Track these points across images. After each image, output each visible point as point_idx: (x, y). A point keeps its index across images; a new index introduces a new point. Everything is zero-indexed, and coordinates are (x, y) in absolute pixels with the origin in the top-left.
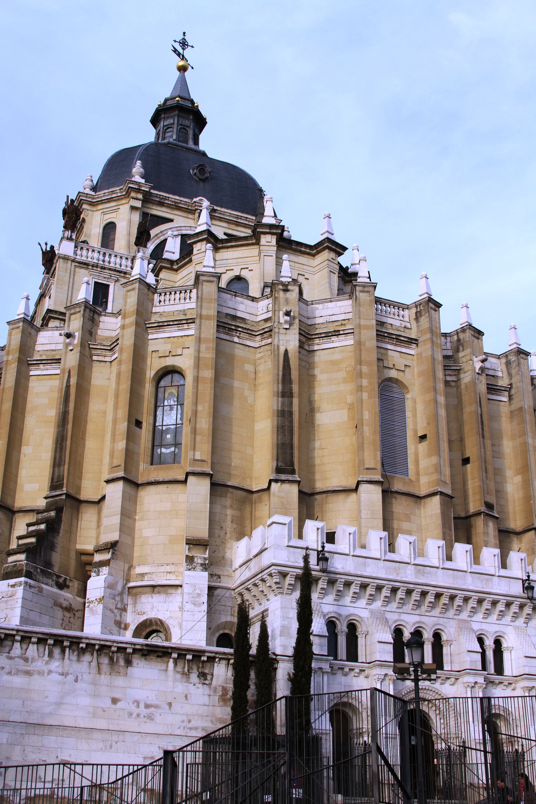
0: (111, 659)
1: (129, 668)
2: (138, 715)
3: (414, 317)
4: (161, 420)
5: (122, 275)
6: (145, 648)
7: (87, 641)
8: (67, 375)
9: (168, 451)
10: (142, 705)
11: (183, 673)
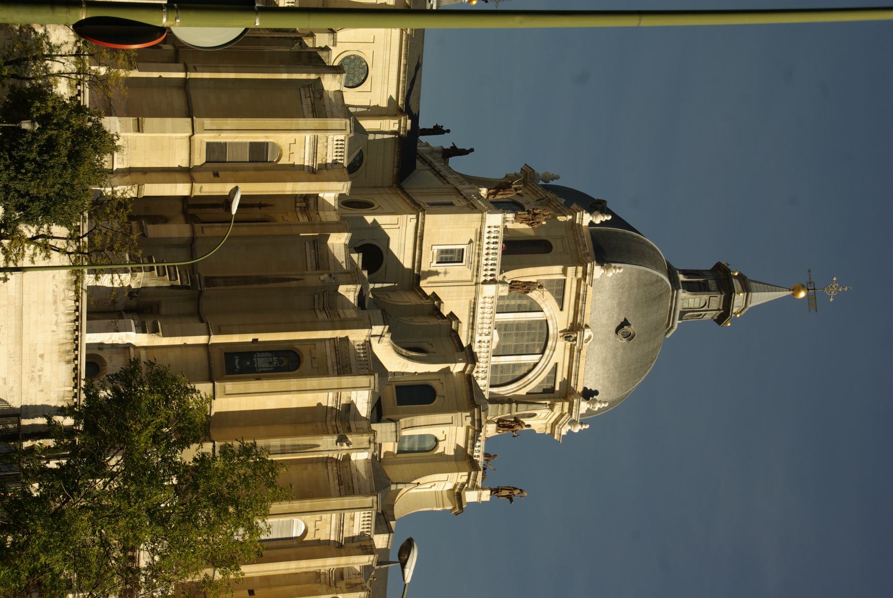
0: (69, 351)
1: (64, 363)
2: (33, 372)
3: (362, 545)
4: (261, 356)
5: (475, 274)
6: (79, 371)
7: (80, 335)
8: (299, 277)
9: (237, 364)
10: (40, 373)
11: (64, 397)
